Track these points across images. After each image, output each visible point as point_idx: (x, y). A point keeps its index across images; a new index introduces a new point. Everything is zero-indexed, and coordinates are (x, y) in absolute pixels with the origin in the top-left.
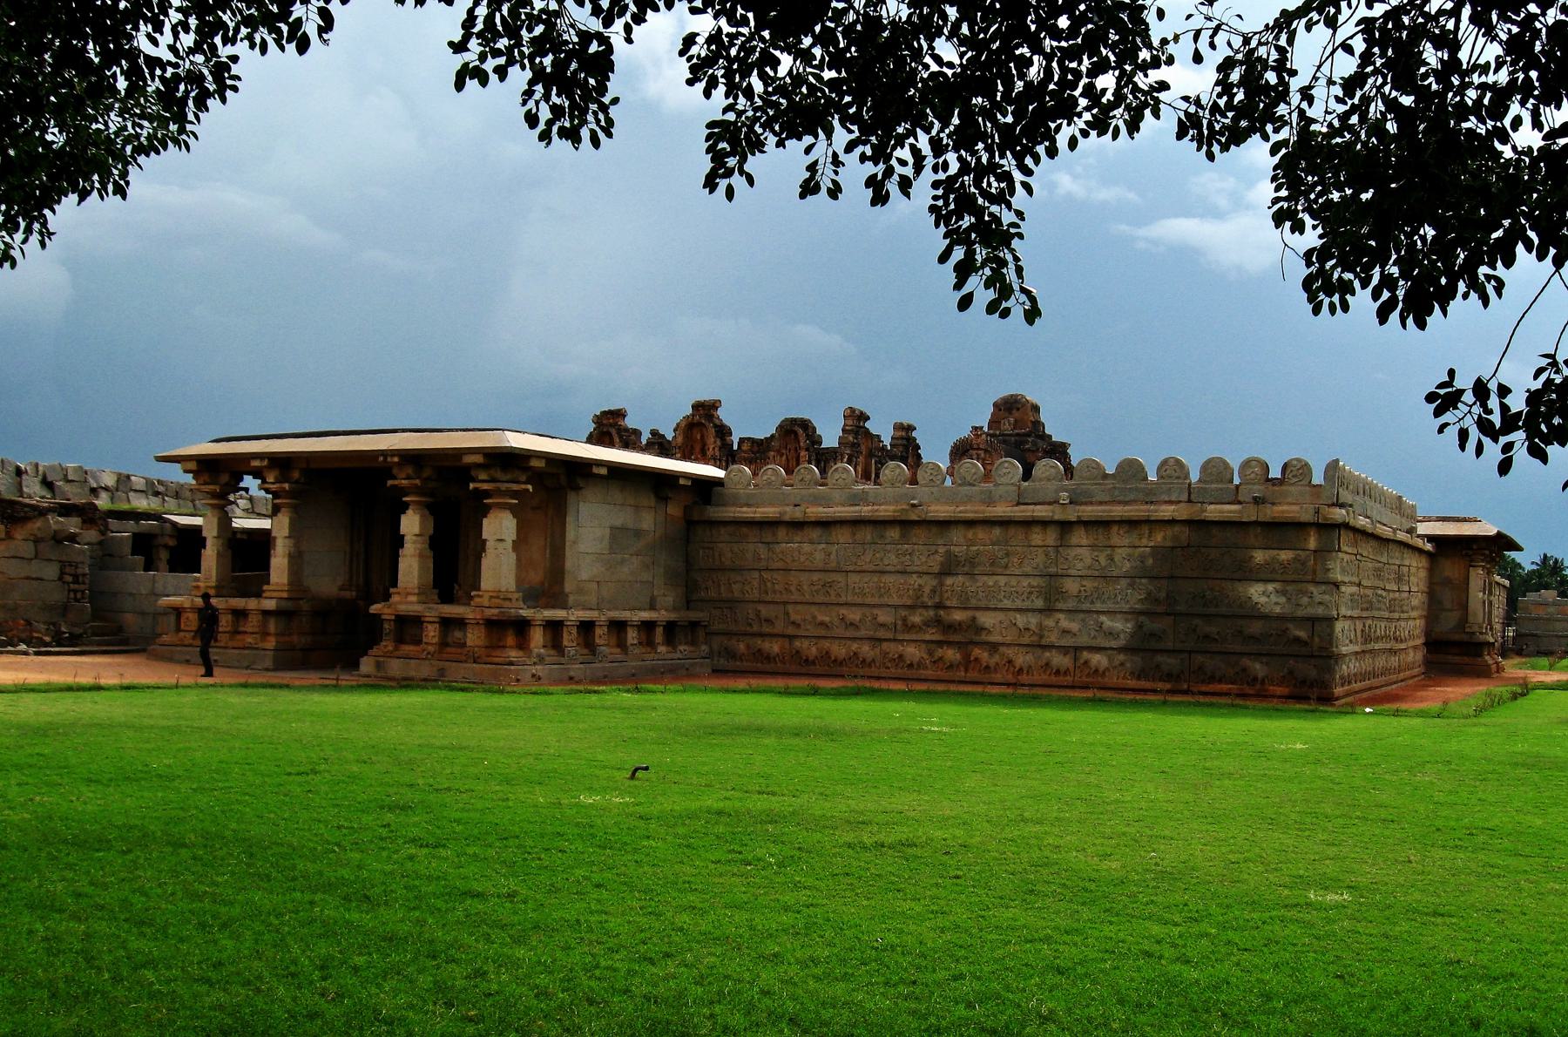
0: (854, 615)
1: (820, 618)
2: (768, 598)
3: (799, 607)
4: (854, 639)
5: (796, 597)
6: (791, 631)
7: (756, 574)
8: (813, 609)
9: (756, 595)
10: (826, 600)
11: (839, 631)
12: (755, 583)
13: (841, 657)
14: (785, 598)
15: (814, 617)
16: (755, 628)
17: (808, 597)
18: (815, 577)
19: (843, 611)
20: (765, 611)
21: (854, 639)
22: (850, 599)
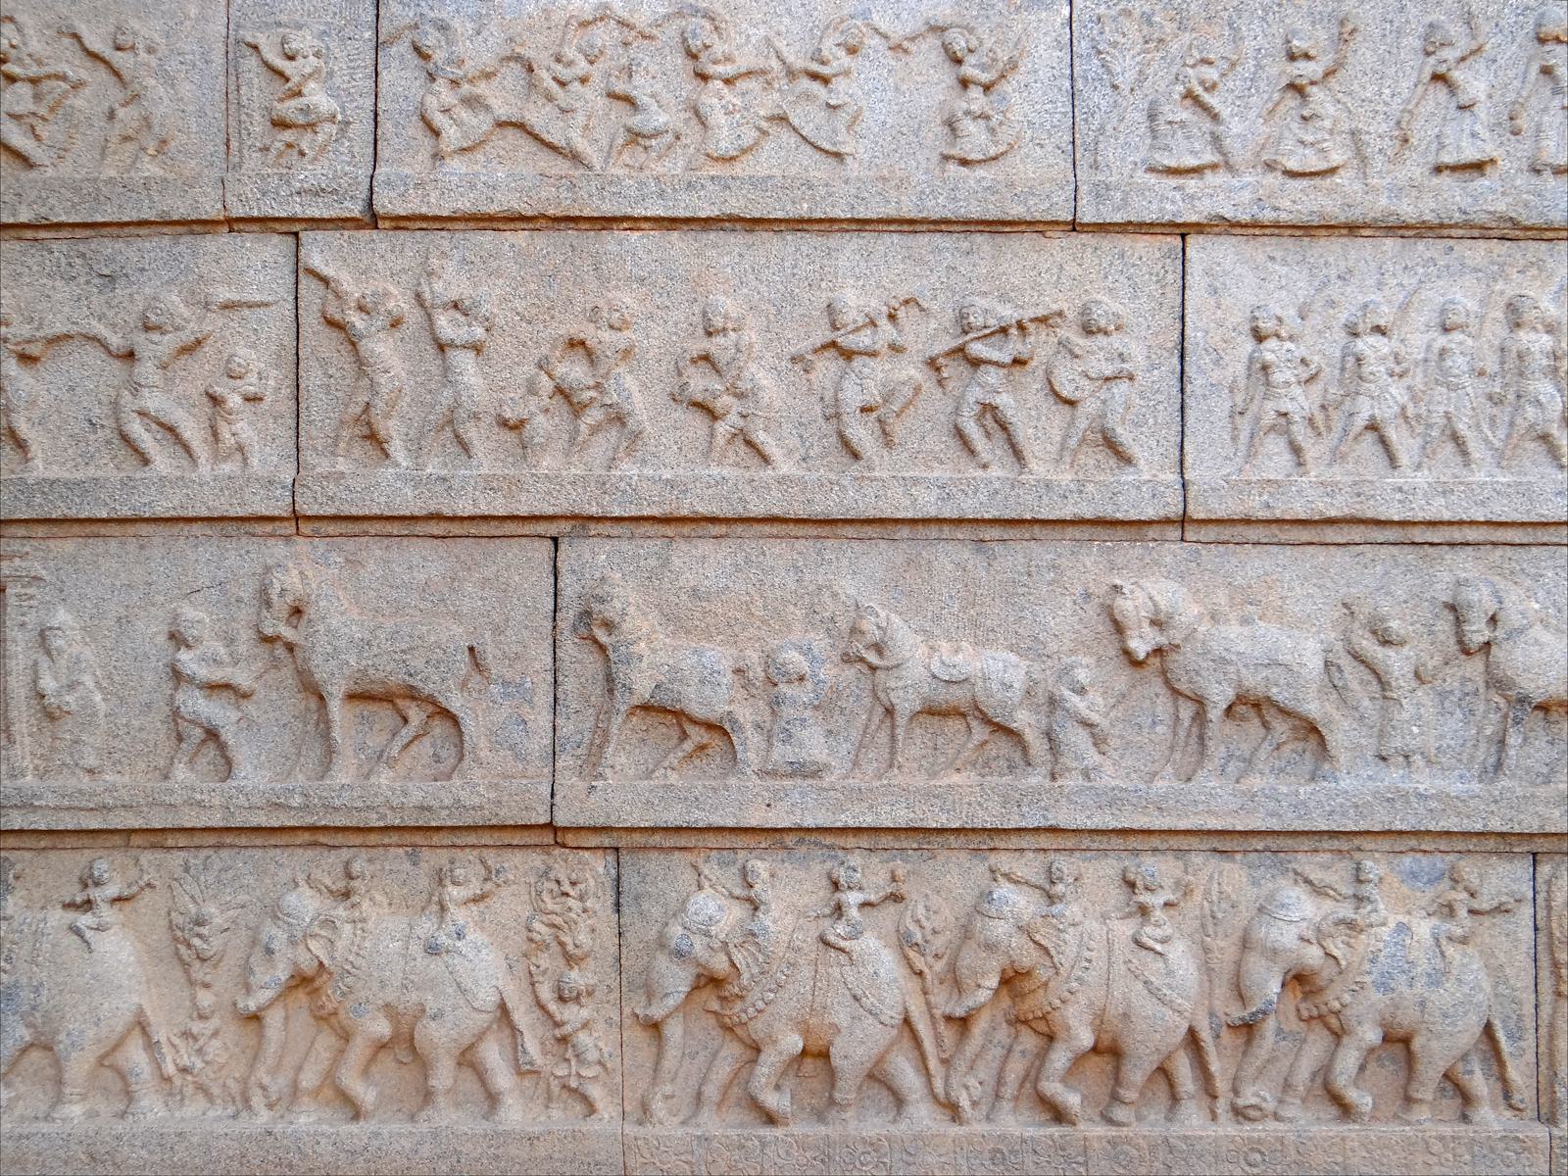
0: (1273, 625)
1: (925, 658)
2: (392, 487)
3: (703, 563)
4: (1274, 844)
5: (674, 466)
6: (633, 785)
7: (259, 264)
8: (855, 576)
9: (258, 463)
10: (986, 487)
11: (1123, 770)
12: (254, 353)
13: (1155, 1030)
14: (556, 478)
15: (867, 658)
16: (261, 778)
17: (796, 475)
18: (858, 280)
19: (1157, 588)
20: (357, 610)
21: (1274, 844)
22: (1219, 478)
